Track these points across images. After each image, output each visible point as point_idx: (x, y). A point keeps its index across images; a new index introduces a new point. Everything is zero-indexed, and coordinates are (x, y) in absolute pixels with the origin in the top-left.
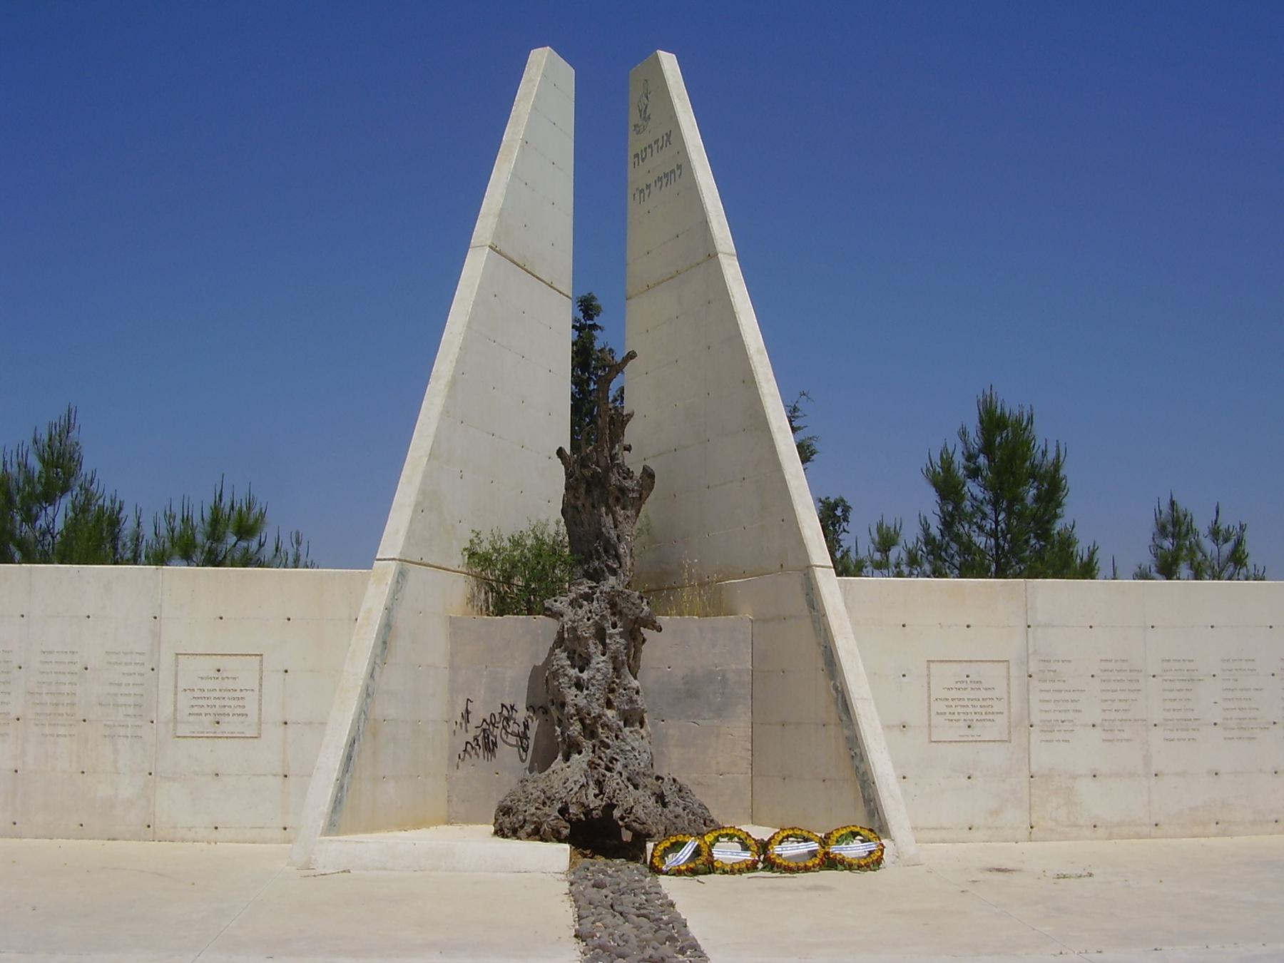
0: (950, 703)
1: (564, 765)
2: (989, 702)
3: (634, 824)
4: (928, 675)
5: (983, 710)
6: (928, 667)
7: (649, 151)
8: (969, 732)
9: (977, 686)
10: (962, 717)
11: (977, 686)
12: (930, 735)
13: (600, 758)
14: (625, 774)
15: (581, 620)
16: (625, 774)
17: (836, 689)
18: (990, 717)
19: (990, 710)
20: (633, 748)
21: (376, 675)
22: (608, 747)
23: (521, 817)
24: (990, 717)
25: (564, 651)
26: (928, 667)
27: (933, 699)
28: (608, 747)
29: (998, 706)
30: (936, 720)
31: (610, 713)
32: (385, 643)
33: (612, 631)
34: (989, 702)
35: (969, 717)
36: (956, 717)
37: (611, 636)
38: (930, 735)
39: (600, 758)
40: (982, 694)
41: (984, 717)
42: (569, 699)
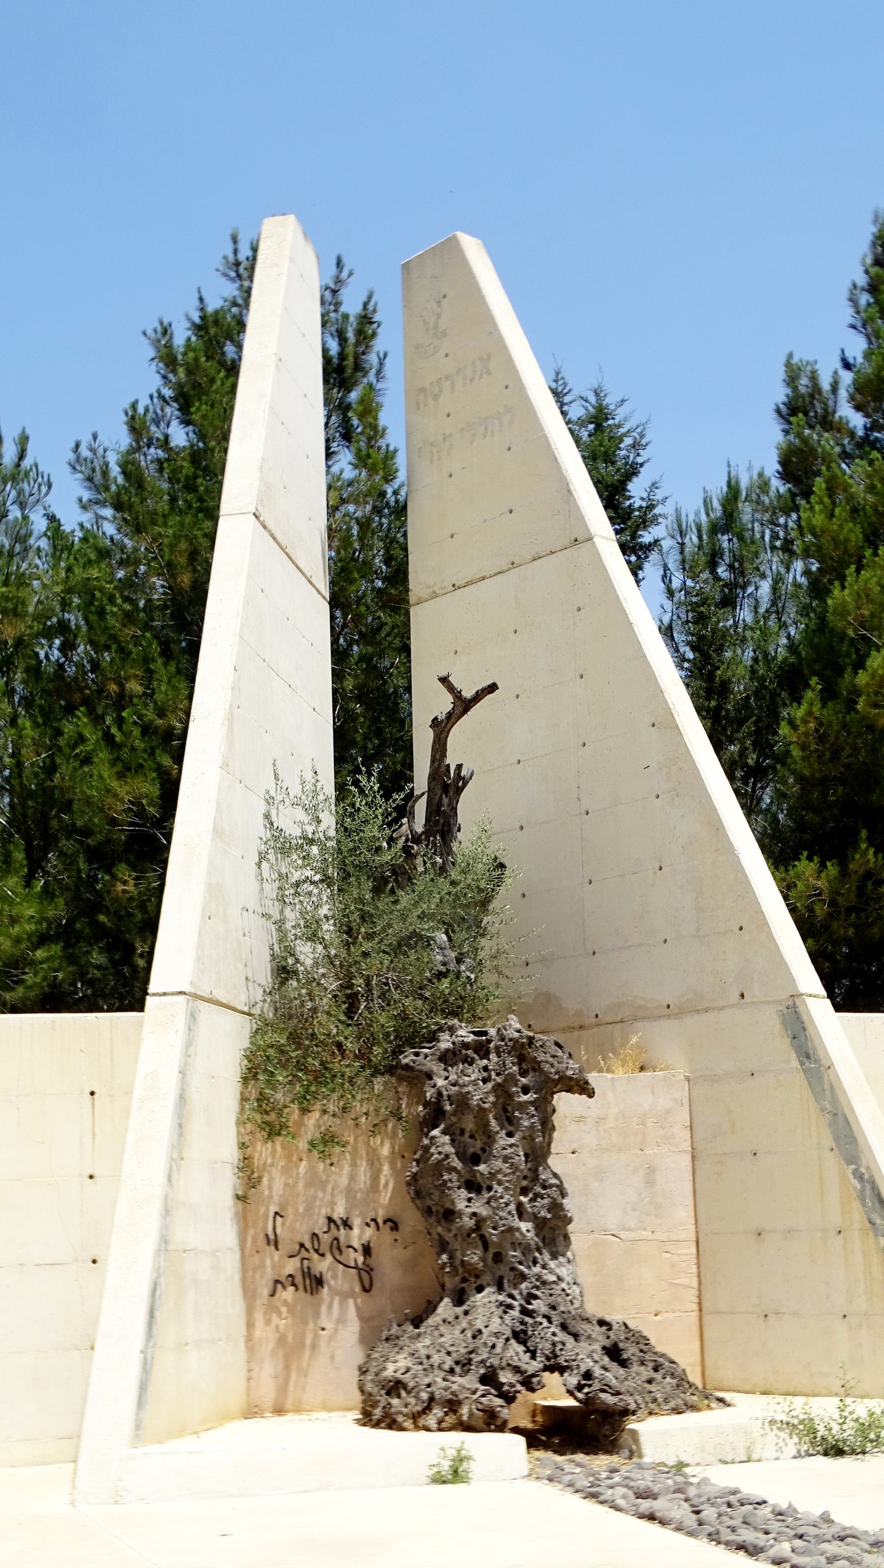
1: (459, 1310)
3: (603, 1396)
7: (447, 384)
13: (511, 1296)
14: (556, 1320)
15: (474, 1083)
16: (556, 1320)
17: (860, 1178)
20: (560, 1279)
21: (175, 1176)
22: (523, 1277)
23: (424, 1396)
25: (444, 1132)
31: (524, 1226)
32: (180, 1126)
33: (524, 1098)
37: (522, 1106)
39: (511, 1296)
42: (461, 1205)
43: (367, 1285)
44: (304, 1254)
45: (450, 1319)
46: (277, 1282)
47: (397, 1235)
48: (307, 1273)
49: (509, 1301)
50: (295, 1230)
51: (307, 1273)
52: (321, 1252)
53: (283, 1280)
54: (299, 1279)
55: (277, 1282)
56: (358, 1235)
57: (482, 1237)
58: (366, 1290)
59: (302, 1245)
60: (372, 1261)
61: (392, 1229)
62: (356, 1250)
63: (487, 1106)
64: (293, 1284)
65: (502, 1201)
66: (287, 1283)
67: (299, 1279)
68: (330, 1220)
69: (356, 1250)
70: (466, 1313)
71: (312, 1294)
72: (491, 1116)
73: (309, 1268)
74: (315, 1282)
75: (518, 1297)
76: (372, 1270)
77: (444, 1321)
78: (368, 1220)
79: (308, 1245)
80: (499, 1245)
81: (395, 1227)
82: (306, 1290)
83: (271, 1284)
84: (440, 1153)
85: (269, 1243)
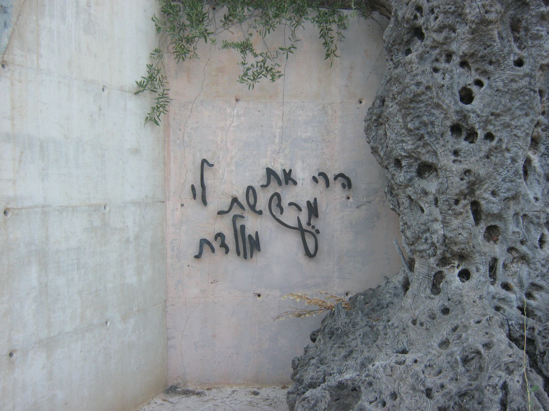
13: (506, 287)
28: (523, 258)
43: (312, 251)
44: (236, 211)
45: (423, 318)
46: (204, 242)
47: (350, 193)
48: (240, 232)
49: (503, 293)
50: (228, 183)
51: (240, 232)
52: (258, 208)
53: (210, 238)
54: (230, 240)
55: (204, 242)
56: (303, 191)
57: (475, 205)
58: (309, 255)
59: (235, 200)
60: (318, 224)
61: (344, 186)
62: (300, 209)
63: (492, 16)
64: (223, 245)
65: (507, 155)
66: (216, 245)
67: (230, 240)
68: (270, 172)
69: (300, 209)
70: (446, 311)
71: (245, 257)
72: (496, 33)
73: (243, 227)
74: (249, 246)
75: (516, 289)
76: (318, 232)
77: (414, 322)
78: (316, 175)
79: (242, 200)
80: (499, 216)
81: (347, 182)
82: (239, 254)
83: (197, 242)
84: (418, 84)
85: (194, 196)
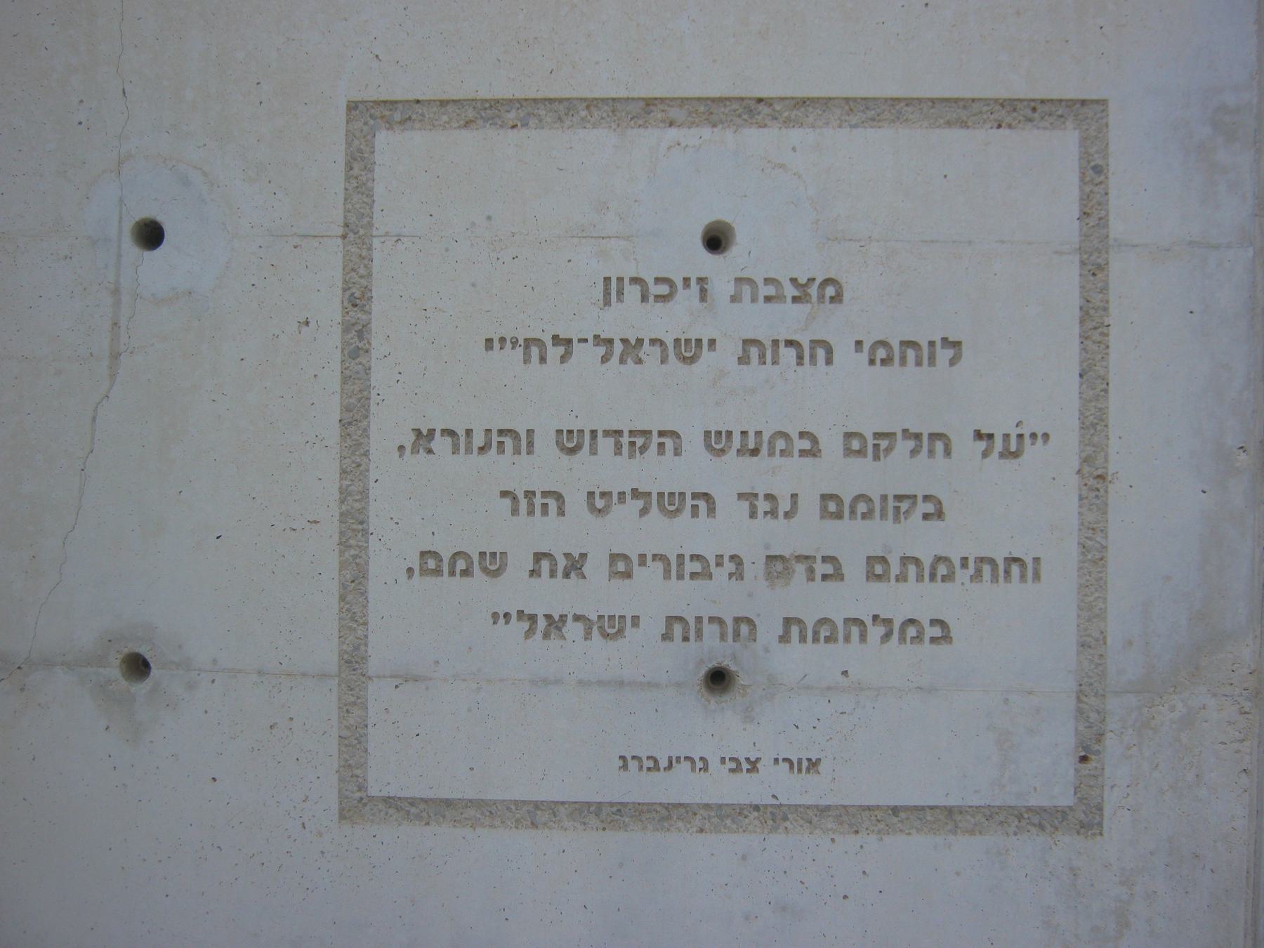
0: (545, 468)
2: (900, 472)
4: (357, 231)
5: (854, 540)
6: (359, 163)
8: (716, 729)
9: (787, 320)
10: (651, 595)
11: (787, 320)
12: (353, 742)
18: (903, 600)
19: (921, 539)
24: (903, 600)
26: (359, 163)
27: (389, 425)
29: (1016, 507)
30: (406, 615)
34: (900, 472)
35: (719, 596)
36: (596, 594)
38: (353, 742)
40: (844, 396)
41: (854, 597)
